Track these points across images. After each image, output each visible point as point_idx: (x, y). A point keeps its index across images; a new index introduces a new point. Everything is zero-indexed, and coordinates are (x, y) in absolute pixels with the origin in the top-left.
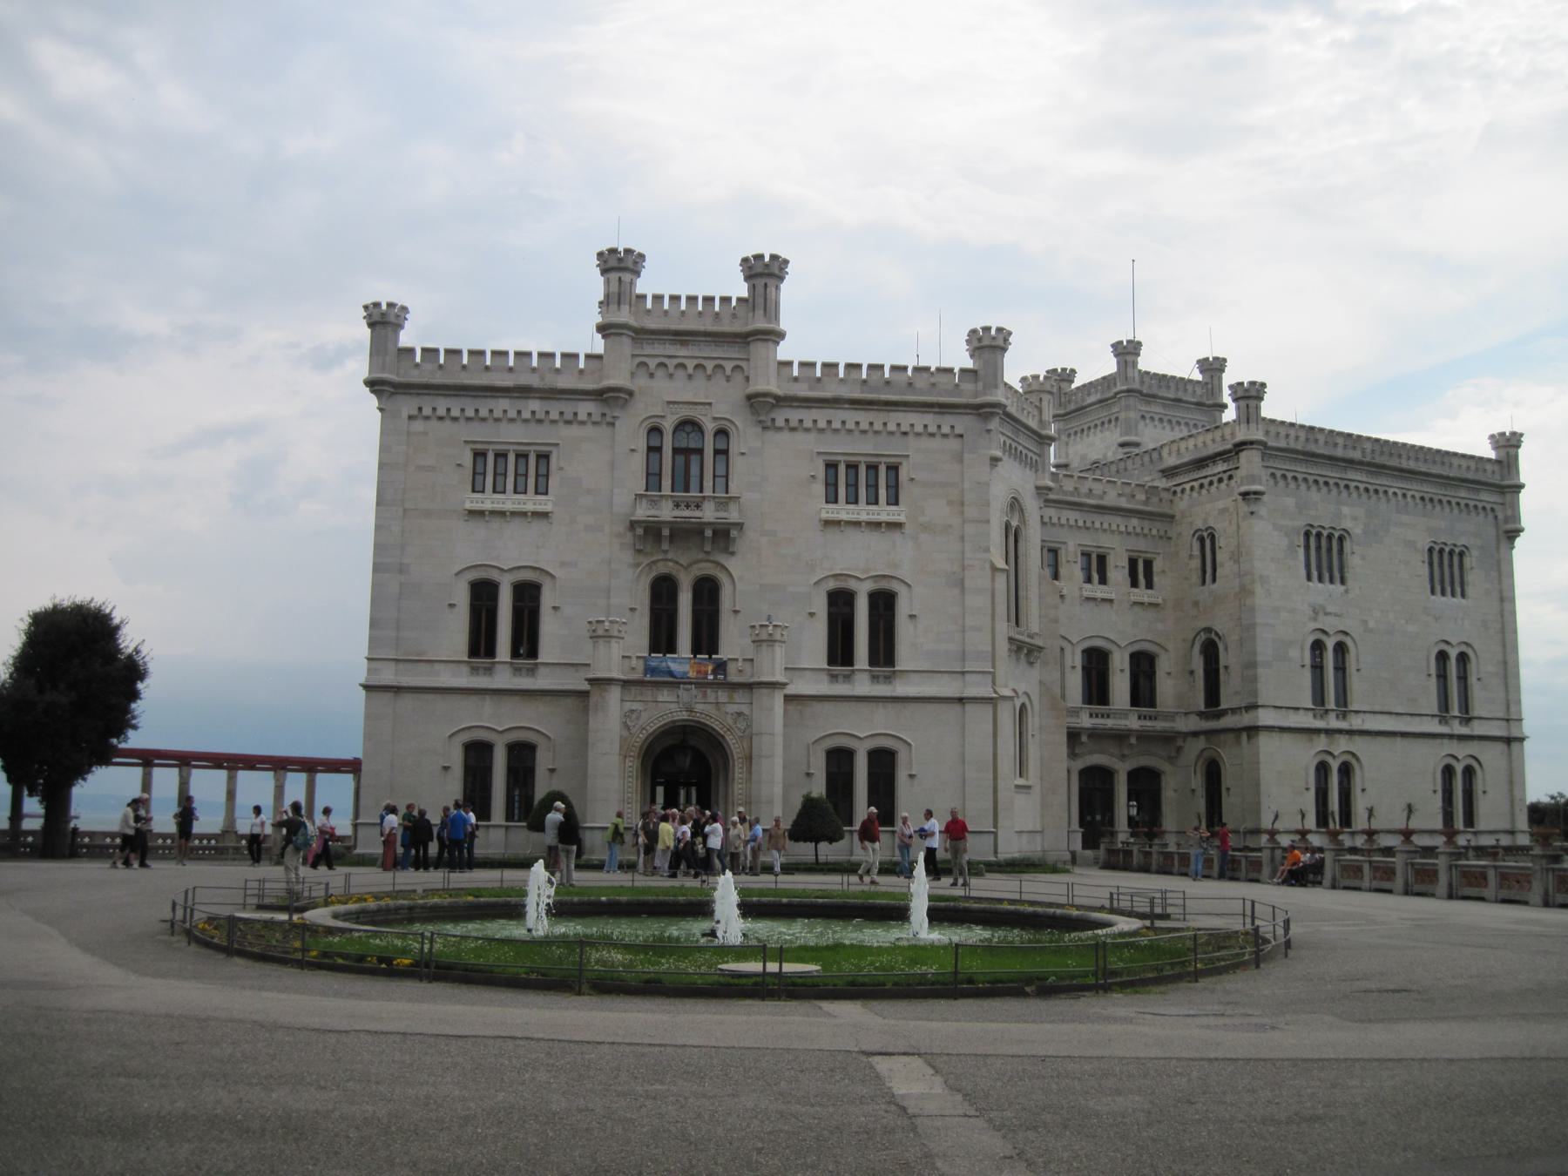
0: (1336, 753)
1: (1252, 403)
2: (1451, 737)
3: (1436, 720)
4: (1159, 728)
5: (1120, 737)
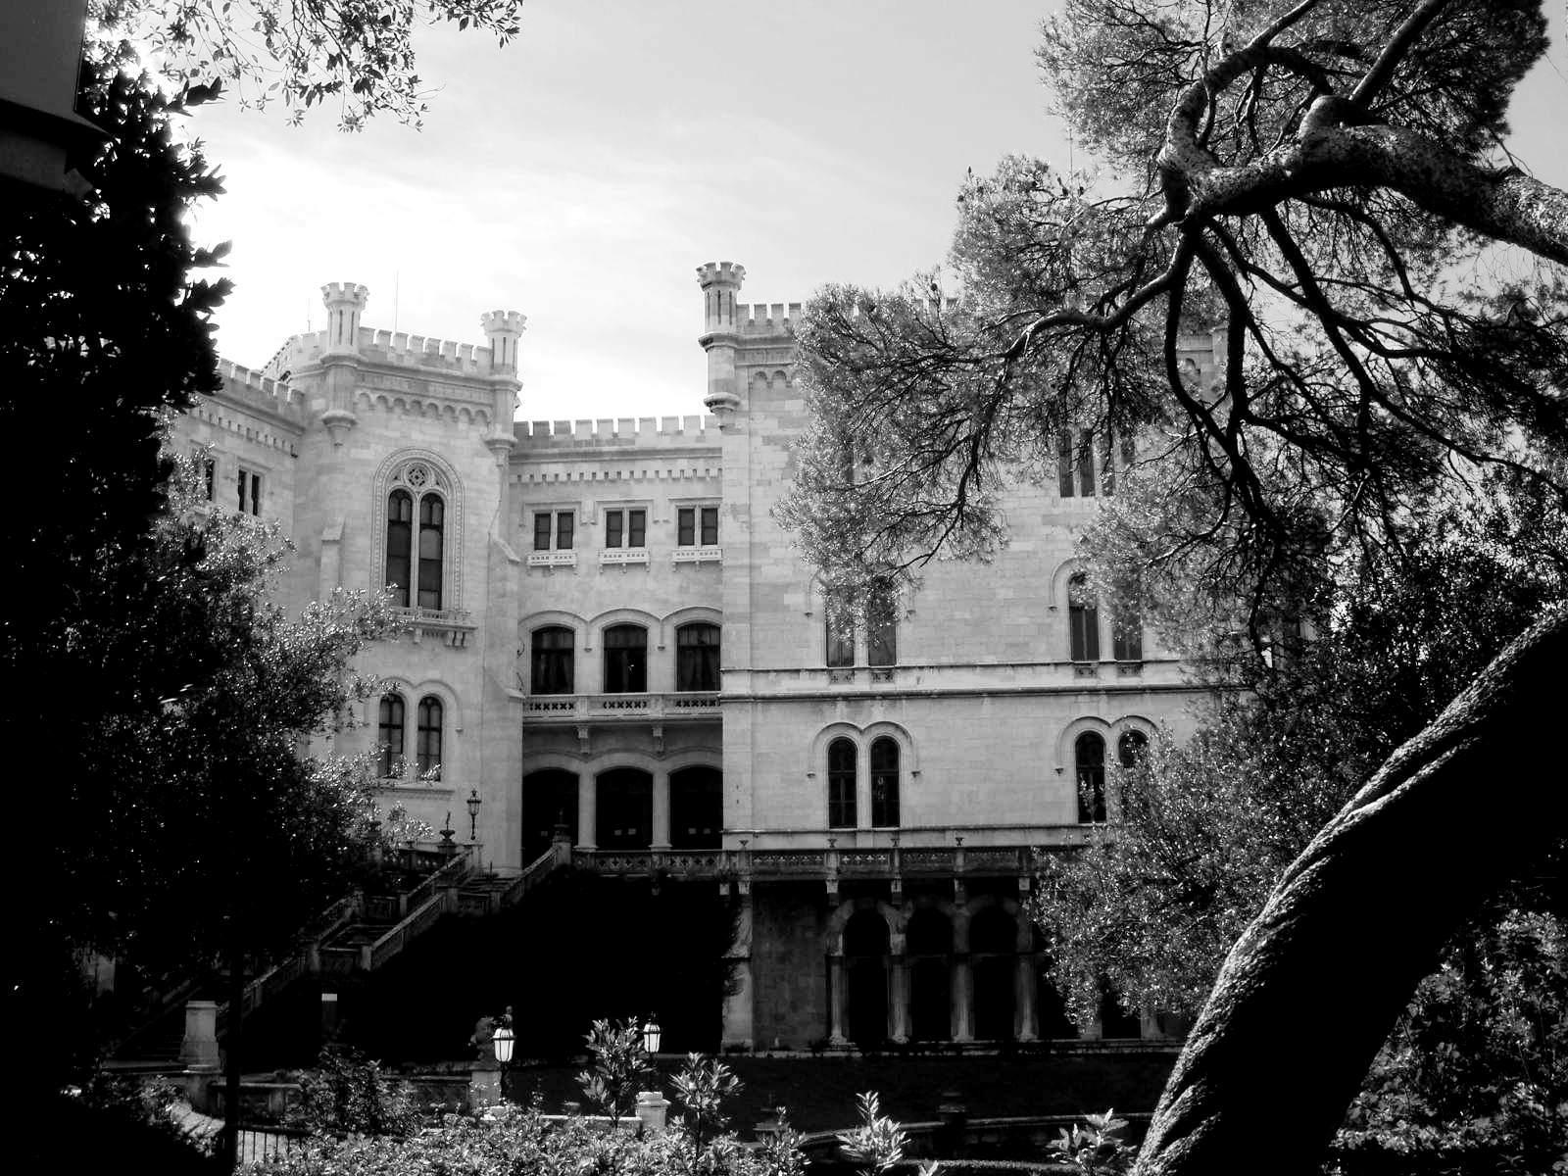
0: (862, 727)
1: (712, 290)
2: (1093, 692)
3: (1070, 671)
4: (694, 716)
5: (645, 728)
